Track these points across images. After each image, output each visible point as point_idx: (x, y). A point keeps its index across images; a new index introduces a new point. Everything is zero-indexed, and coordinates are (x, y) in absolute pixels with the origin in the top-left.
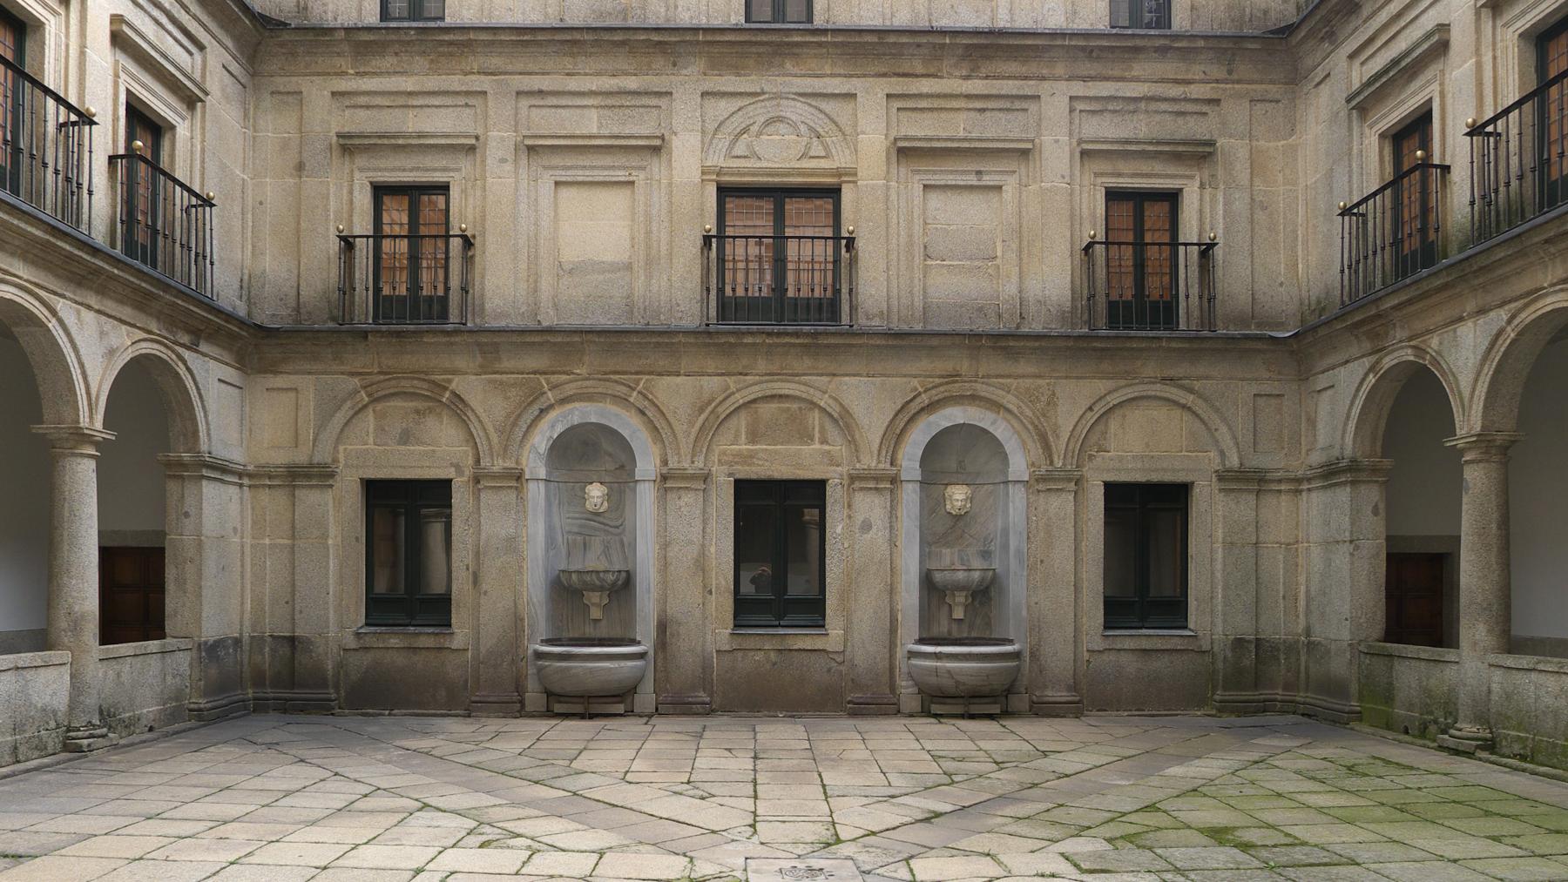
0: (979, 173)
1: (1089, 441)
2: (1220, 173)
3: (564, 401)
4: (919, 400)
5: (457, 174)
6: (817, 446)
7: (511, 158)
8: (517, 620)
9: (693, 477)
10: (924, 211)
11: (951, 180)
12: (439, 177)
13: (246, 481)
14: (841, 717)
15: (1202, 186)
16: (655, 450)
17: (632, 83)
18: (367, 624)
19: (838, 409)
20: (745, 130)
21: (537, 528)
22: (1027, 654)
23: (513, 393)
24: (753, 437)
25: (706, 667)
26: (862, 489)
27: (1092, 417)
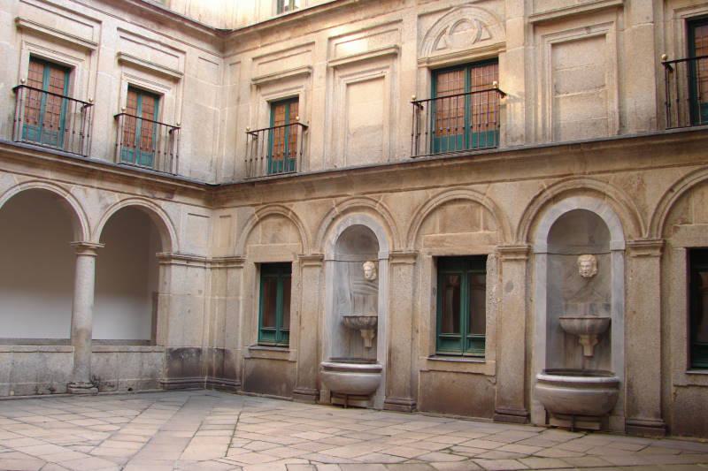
0: (588, 28)
1: (671, 215)
6: (482, 232)
7: (324, 74)
8: (318, 346)
9: (406, 256)
11: (569, 37)
12: (294, 93)
13: (208, 265)
14: (489, 422)
17: (381, 20)
18: (259, 345)
19: (492, 205)
21: (329, 291)
22: (624, 386)
23: (319, 209)
24: (444, 229)
25: (412, 382)
26: (507, 260)
27: (672, 198)
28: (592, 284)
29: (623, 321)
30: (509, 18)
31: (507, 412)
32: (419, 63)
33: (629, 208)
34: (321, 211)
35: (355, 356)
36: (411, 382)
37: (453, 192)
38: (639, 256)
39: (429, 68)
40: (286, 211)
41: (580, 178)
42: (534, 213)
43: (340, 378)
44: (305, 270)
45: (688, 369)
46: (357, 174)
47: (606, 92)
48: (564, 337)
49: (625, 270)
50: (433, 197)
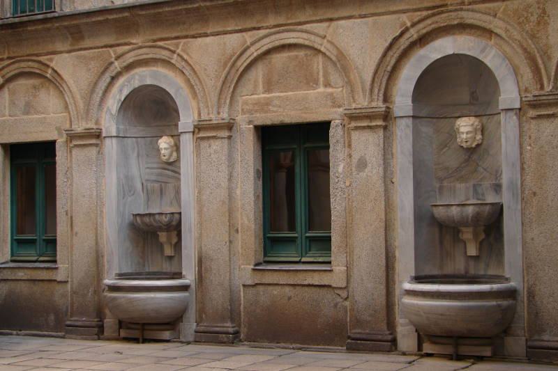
3: (129, 67)
4: (407, 35)
6: (321, 89)
9: (217, 127)
16: (194, 104)
19: (335, 52)
22: (524, 295)
23: (93, 64)
26: (357, 128)
28: (475, 157)
29: (519, 207)
31: (364, 336)
33: (525, 50)
34: (95, 66)
35: (151, 270)
36: (231, 301)
37: (278, 36)
38: (540, 117)
40: (43, 67)
41: (456, 10)
42: (393, 61)
43: (131, 301)
44: (75, 151)
48: (438, 233)
49: (521, 136)
50: (252, 44)
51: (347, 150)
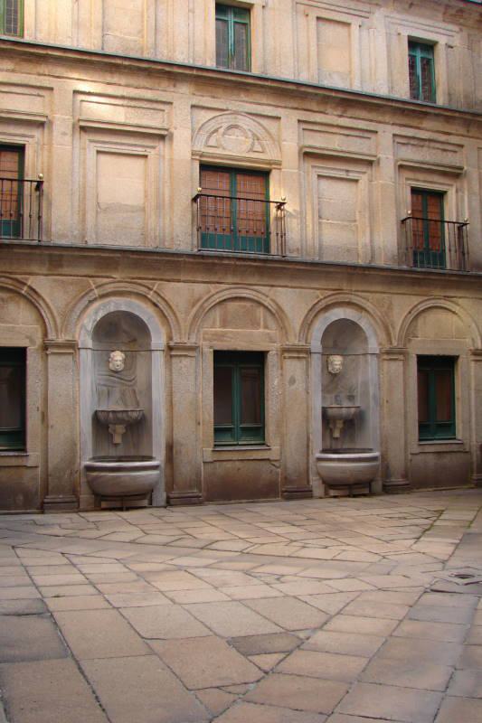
0: (347, 171)
1: (409, 332)
2: (466, 186)
5: (32, 141)
6: (261, 330)
7: (69, 131)
8: (73, 447)
10: (318, 190)
15: (457, 191)
16: (163, 331)
17: (149, 94)
19: (275, 307)
20: (216, 131)
24: (225, 323)
26: (290, 358)
28: (336, 379)
30: (285, 140)
32: (193, 155)
33: (383, 322)
35: (103, 454)
38: (391, 359)
39: (200, 161)
40: (18, 285)
45: (420, 440)
46: (135, 256)
47: (357, 227)
51: (280, 372)
